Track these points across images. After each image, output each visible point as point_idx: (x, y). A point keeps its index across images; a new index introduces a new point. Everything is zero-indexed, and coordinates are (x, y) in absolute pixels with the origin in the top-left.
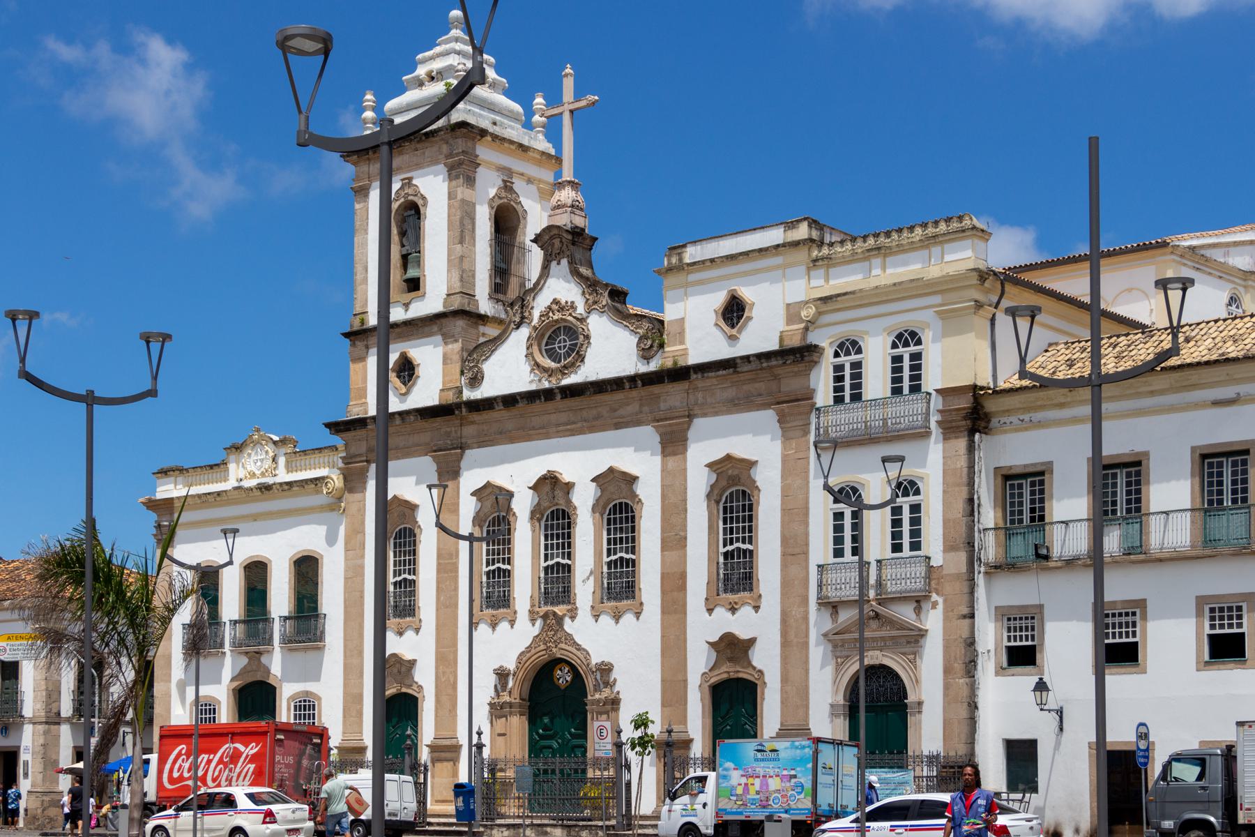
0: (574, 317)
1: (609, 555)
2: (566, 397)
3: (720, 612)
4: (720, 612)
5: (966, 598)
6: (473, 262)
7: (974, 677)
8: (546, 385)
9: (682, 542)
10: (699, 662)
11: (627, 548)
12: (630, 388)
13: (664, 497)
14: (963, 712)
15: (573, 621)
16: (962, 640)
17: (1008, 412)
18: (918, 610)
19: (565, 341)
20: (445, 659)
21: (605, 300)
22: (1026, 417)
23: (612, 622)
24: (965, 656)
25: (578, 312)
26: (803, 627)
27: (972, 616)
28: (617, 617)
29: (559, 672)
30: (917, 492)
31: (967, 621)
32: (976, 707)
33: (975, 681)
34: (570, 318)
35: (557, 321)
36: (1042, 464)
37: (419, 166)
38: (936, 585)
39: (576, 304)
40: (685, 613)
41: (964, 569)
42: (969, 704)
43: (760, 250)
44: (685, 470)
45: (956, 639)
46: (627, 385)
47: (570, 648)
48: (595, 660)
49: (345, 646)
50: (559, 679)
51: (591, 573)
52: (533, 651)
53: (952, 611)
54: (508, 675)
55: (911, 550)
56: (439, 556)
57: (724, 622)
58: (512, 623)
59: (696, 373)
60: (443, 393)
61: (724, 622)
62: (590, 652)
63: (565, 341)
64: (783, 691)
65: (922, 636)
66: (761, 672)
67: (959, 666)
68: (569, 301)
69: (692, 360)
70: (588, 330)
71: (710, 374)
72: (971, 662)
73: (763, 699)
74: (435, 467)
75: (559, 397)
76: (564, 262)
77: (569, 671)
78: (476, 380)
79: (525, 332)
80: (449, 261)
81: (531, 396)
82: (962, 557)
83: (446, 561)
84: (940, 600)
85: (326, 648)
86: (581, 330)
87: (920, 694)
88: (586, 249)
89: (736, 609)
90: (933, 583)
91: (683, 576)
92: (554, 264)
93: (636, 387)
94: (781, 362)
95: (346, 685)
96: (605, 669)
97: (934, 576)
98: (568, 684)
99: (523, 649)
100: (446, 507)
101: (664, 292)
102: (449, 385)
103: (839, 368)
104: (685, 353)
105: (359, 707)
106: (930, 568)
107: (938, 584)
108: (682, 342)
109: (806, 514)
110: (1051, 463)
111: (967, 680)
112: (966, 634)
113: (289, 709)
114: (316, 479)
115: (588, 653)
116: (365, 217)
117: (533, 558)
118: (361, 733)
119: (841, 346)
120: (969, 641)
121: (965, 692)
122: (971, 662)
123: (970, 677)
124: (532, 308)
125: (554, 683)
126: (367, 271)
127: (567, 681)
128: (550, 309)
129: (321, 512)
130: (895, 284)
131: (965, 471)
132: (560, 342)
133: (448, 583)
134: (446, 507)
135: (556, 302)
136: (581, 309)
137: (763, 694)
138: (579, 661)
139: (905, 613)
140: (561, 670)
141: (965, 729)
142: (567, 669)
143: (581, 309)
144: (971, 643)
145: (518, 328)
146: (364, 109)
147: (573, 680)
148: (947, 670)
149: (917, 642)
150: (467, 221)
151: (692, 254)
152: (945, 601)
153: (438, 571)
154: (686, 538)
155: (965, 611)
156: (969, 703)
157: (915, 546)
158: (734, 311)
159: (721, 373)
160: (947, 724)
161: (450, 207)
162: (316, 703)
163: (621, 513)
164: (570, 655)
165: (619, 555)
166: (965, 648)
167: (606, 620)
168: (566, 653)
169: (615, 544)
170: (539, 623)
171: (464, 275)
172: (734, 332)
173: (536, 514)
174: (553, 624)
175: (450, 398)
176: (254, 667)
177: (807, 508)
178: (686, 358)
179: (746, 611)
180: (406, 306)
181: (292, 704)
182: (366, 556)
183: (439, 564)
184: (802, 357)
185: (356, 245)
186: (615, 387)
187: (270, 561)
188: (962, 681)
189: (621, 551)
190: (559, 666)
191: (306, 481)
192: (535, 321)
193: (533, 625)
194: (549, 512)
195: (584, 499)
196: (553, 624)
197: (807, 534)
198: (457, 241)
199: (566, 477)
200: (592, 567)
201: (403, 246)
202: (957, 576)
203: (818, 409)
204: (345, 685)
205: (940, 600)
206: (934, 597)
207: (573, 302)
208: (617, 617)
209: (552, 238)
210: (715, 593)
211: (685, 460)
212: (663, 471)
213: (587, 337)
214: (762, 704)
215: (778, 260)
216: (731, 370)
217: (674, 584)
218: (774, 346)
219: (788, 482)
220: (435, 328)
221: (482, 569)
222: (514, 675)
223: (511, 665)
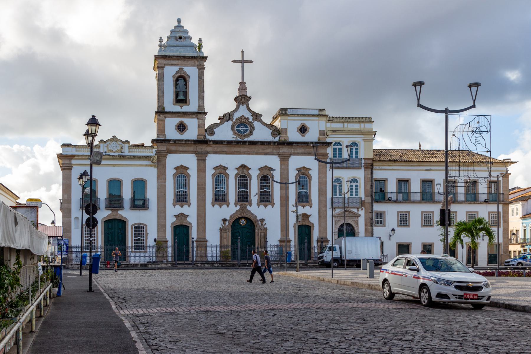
2: (250, 144)
5: (371, 208)
8: (239, 139)
10: (292, 220)
12: (273, 145)
17: (377, 165)
18: (358, 211)
22: (381, 167)
23: (264, 207)
26: (325, 213)
28: (266, 207)
30: (357, 182)
31: (371, 214)
35: (242, 122)
36: (385, 178)
37: (186, 65)
39: (249, 118)
41: (370, 201)
43: (313, 115)
46: (272, 144)
47: (250, 215)
48: (259, 218)
49: (158, 210)
51: (257, 194)
55: (356, 196)
56: (198, 185)
58: (228, 206)
59: (295, 144)
60: (199, 136)
61: (301, 210)
63: (243, 128)
64: (319, 229)
67: (369, 224)
68: (247, 117)
69: (290, 140)
71: (300, 145)
74: (196, 158)
75: (247, 144)
76: (245, 105)
78: (212, 134)
79: (230, 123)
80: (199, 97)
81: (238, 142)
82: (370, 198)
84: (364, 208)
92: (241, 106)
93: (275, 145)
94: (322, 145)
96: (262, 220)
99: (232, 214)
100: (201, 170)
103: (335, 149)
104: (288, 138)
105: (164, 229)
108: (286, 135)
110: (387, 178)
112: (371, 217)
113: (132, 228)
114: (147, 156)
116: (162, 77)
119: (336, 143)
121: (370, 230)
126: (163, 93)
129: (146, 166)
130: (354, 131)
131: (370, 178)
132: (241, 128)
134: (201, 170)
135: (243, 116)
136: (251, 119)
139: (355, 210)
140: (242, 220)
142: (244, 220)
143: (251, 119)
145: (228, 121)
147: (247, 223)
148: (366, 225)
149: (358, 218)
152: (365, 209)
153: (198, 189)
155: (371, 211)
157: (357, 195)
158: (303, 130)
159: (303, 145)
161: (199, 81)
162: (145, 227)
163: (243, 178)
165: (264, 190)
167: (262, 207)
169: (263, 186)
170: (238, 207)
172: (303, 134)
173: (236, 176)
174: (243, 208)
175: (202, 138)
176: (115, 214)
178: (288, 139)
179: (307, 207)
181: (133, 227)
184: (328, 145)
186: (268, 144)
189: (265, 189)
191: (142, 156)
192: (234, 120)
193: (236, 207)
194: (217, 175)
195: (254, 174)
196: (243, 208)
201: (176, 88)
202: (369, 203)
204: (158, 222)
205: (364, 208)
208: (266, 207)
209: (242, 98)
211: (288, 166)
214: (191, 231)
215: (317, 118)
216: (306, 145)
217: (285, 199)
218: (316, 140)
220: (194, 116)
222: (229, 221)
223: (228, 218)
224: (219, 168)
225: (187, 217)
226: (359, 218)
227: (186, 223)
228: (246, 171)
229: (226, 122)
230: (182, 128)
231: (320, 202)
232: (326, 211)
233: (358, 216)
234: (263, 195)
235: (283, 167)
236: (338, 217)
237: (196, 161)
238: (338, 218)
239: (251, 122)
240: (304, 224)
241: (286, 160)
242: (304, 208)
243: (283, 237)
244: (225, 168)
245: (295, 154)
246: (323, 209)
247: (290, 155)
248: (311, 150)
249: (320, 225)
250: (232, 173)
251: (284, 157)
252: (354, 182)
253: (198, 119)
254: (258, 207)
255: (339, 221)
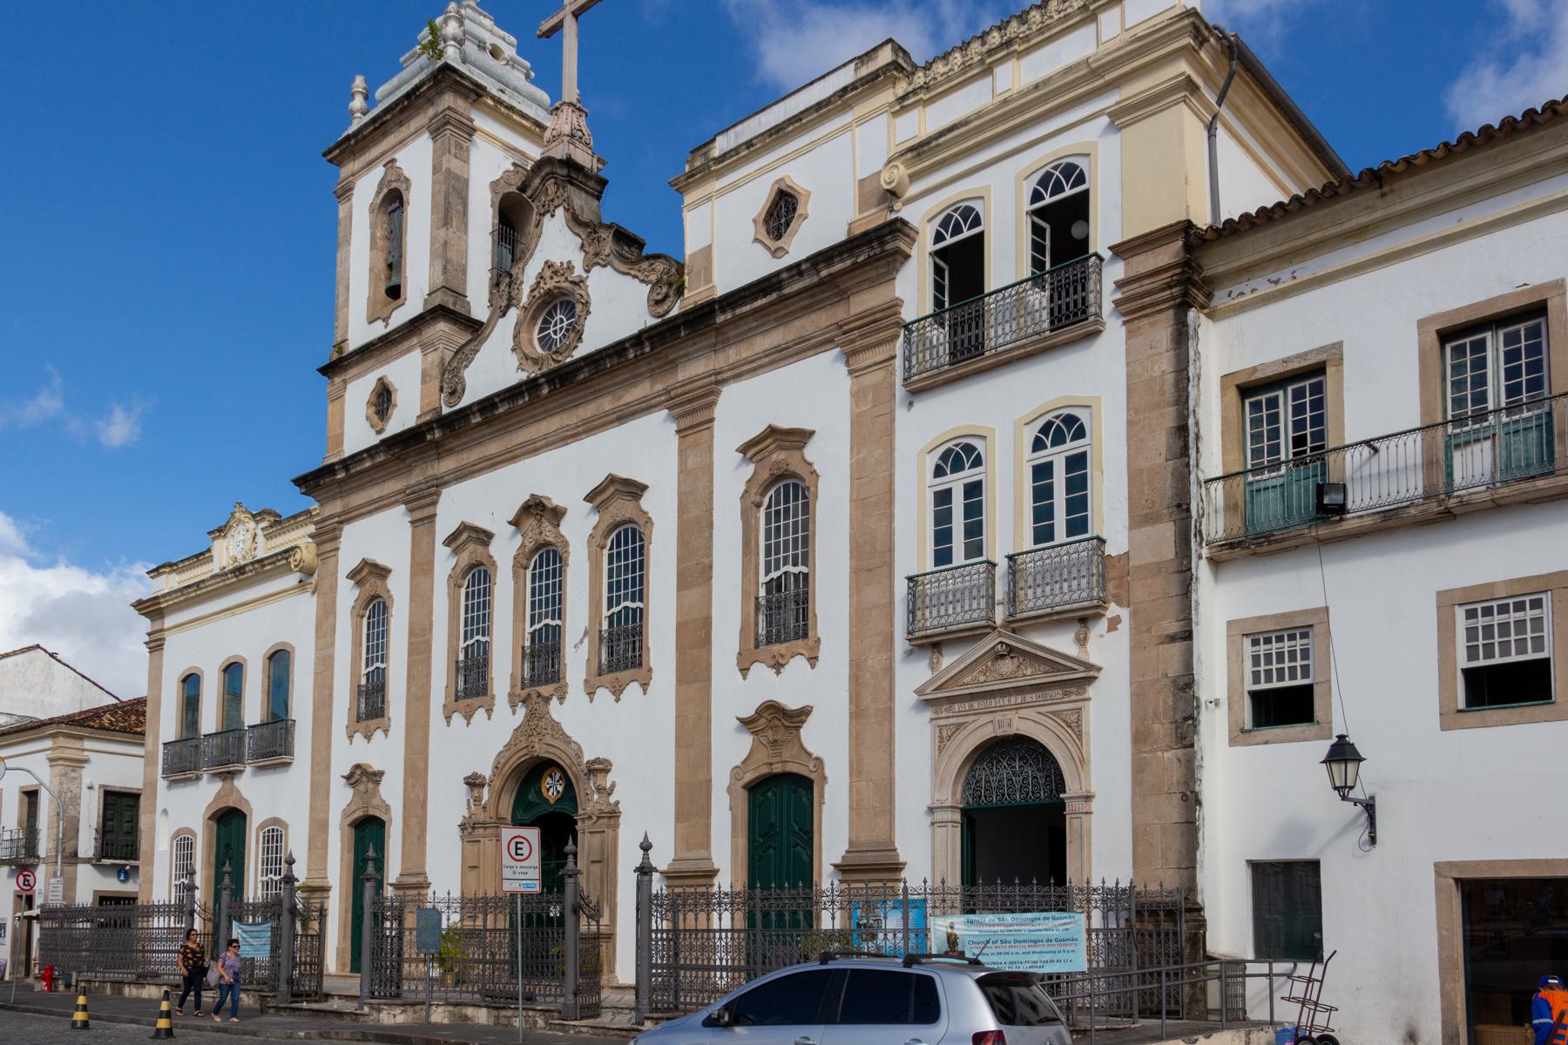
0: (572, 282)
1: (610, 606)
3: (760, 671)
4: (760, 671)
6: (464, 253)
7: (1192, 746)
9: (706, 572)
11: (633, 593)
13: (682, 509)
14: (1172, 811)
15: (561, 703)
16: (1168, 681)
19: (562, 321)
20: (416, 770)
21: (608, 246)
24: (1175, 709)
25: (576, 274)
27: (1187, 636)
28: (617, 692)
29: (549, 780)
31: (1177, 647)
32: (1198, 802)
33: (1195, 752)
34: (566, 285)
38: (1116, 588)
39: (574, 263)
40: (709, 680)
42: (1184, 797)
44: (711, 464)
45: (1157, 680)
50: (548, 790)
51: (586, 633)
52: (513, 749)
53: (1149, 630)
54: (482, 785)
57: (765, 685)
58: (489, 711)
59: (723, 311)
61: (765, 685)
62: (583, 747)
65: (1092, 679)
66: (818, 759)
67: (1162, 729)
70: (588, 295)
72: (1186, 719)
73: (822, 803)
77: (561, 778)
78: (455, 393)
83: (419, 639)
84: (1124, 613)
85: (295, 762)
86: (578, 297)
87: (1089, 783)
88: (592, 195)
89: (783, 666)
90: (1111, 587)
91: (707, 623)
95: (312, 810)
97: (1112, 573)
98: (559, 796)
99: (501, 748)
101: (684, 214)
102: (426, 410)
106: (1106, 560)
107: (1119, 586)
109: (890, 502)
111: (1180, 752)
112: (1174, 669)
115: (580, 748)
117: (515, 620)
118: (325, 869)
120: (1181, 682)
121: (1176, 774)
122: (1186, 719)
123: (1185, 747)
124: (522, 282)
125: (542, 794)
127: (558, 792)
128: (541, 277)
133: (420, 668)
135: (549, 265)
137: (822, 795)
138: (568, 761)
139: (1062, 642)
140: (551, 776)
141: (1176, 843)
143: (579, 271)
144: (1185, 684)
146: (352, 97)
147: (565, 789)
148: (1140, 737)
150: (454, 199)
151: (722, 145)
152: (1134, 615)
154: (710, 567)
155: (1174, 627)
156: (1184, 794)
157: (1077, 526)
160: (1140, 835)
164: (558, 752)
166: (1174, 695)
167: (603, 694)
168: (552, 750)
170: (521, 711)
171: (449, 267)
177: (891, 491)
179: (798, 665)
180: (386, 320)
182: (336, 643)
183: (411, 644)
185: (338, 262)
187: (245, 660)
188: (1169, 755)
190: (549, 771)
193: (514, 713)
197: (891, 534)
198: (441, 223)
199: (557, 501)
200: (587, 624)
203: (906, 327)
205: (1124, 613)
206: (1113, 610)
207: (569, 262)
210: (752, 645)
212: (680, 472)
213: (587, 304)
216: (774, 296)
219: (861, 455)
221: (458, 645)
223: (486, 771)
224: (465, 542)
225: (378, 783)
226: (1091, 691)
227: (376, 807)
228: (550, 528)
229: (500, 320)
230: (383, 398)
231: (859, 618)
232: (889, 670)
233: (1080, 678)
234: (626, 630)
235: (690, 463)
236: (952, 700)
237: (408, 529)
238: (956, 707)
239: (579, 283)
240: (778, 769)
241: (701, 417)
242: (778, 673)
243: (682, 856)
244: (482, 536)
245: (741, 372)
246: (874, 661)
247: (718, 381)
248: (813, 317)
249: (856, 770)
250: (505, 549)
251: (688, 407)
252: (1059, 440)
253: (424, 347)
254: (587, 697)
255: (959, 726)
